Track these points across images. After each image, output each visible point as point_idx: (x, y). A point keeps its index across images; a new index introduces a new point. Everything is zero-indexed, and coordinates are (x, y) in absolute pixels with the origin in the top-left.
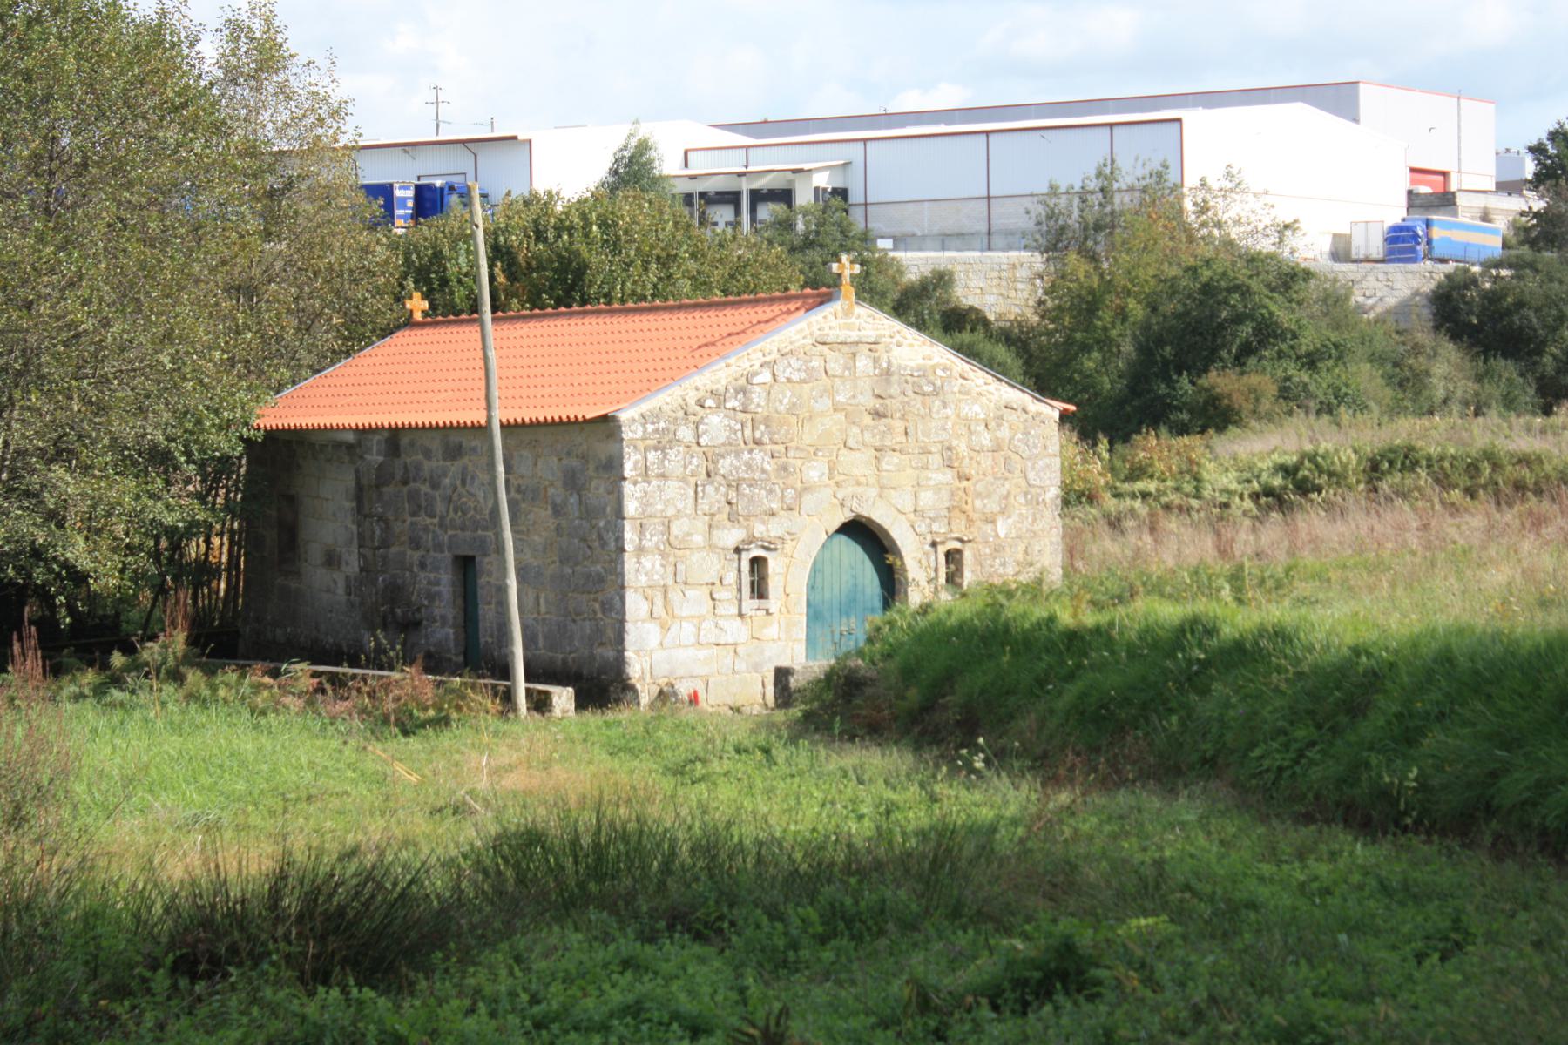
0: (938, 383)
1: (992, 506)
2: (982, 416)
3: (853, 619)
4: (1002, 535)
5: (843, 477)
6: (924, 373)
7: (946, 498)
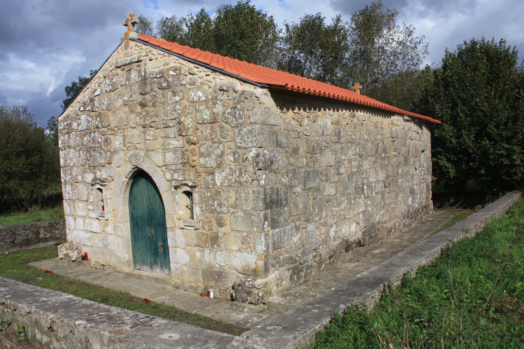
0: (170, 79)
1: (211, 162)
2: (204, 98)
3: (153, 229)
4: (218, 184)
5: (129, 145)
6: (162, 75)
7: (180, 156)
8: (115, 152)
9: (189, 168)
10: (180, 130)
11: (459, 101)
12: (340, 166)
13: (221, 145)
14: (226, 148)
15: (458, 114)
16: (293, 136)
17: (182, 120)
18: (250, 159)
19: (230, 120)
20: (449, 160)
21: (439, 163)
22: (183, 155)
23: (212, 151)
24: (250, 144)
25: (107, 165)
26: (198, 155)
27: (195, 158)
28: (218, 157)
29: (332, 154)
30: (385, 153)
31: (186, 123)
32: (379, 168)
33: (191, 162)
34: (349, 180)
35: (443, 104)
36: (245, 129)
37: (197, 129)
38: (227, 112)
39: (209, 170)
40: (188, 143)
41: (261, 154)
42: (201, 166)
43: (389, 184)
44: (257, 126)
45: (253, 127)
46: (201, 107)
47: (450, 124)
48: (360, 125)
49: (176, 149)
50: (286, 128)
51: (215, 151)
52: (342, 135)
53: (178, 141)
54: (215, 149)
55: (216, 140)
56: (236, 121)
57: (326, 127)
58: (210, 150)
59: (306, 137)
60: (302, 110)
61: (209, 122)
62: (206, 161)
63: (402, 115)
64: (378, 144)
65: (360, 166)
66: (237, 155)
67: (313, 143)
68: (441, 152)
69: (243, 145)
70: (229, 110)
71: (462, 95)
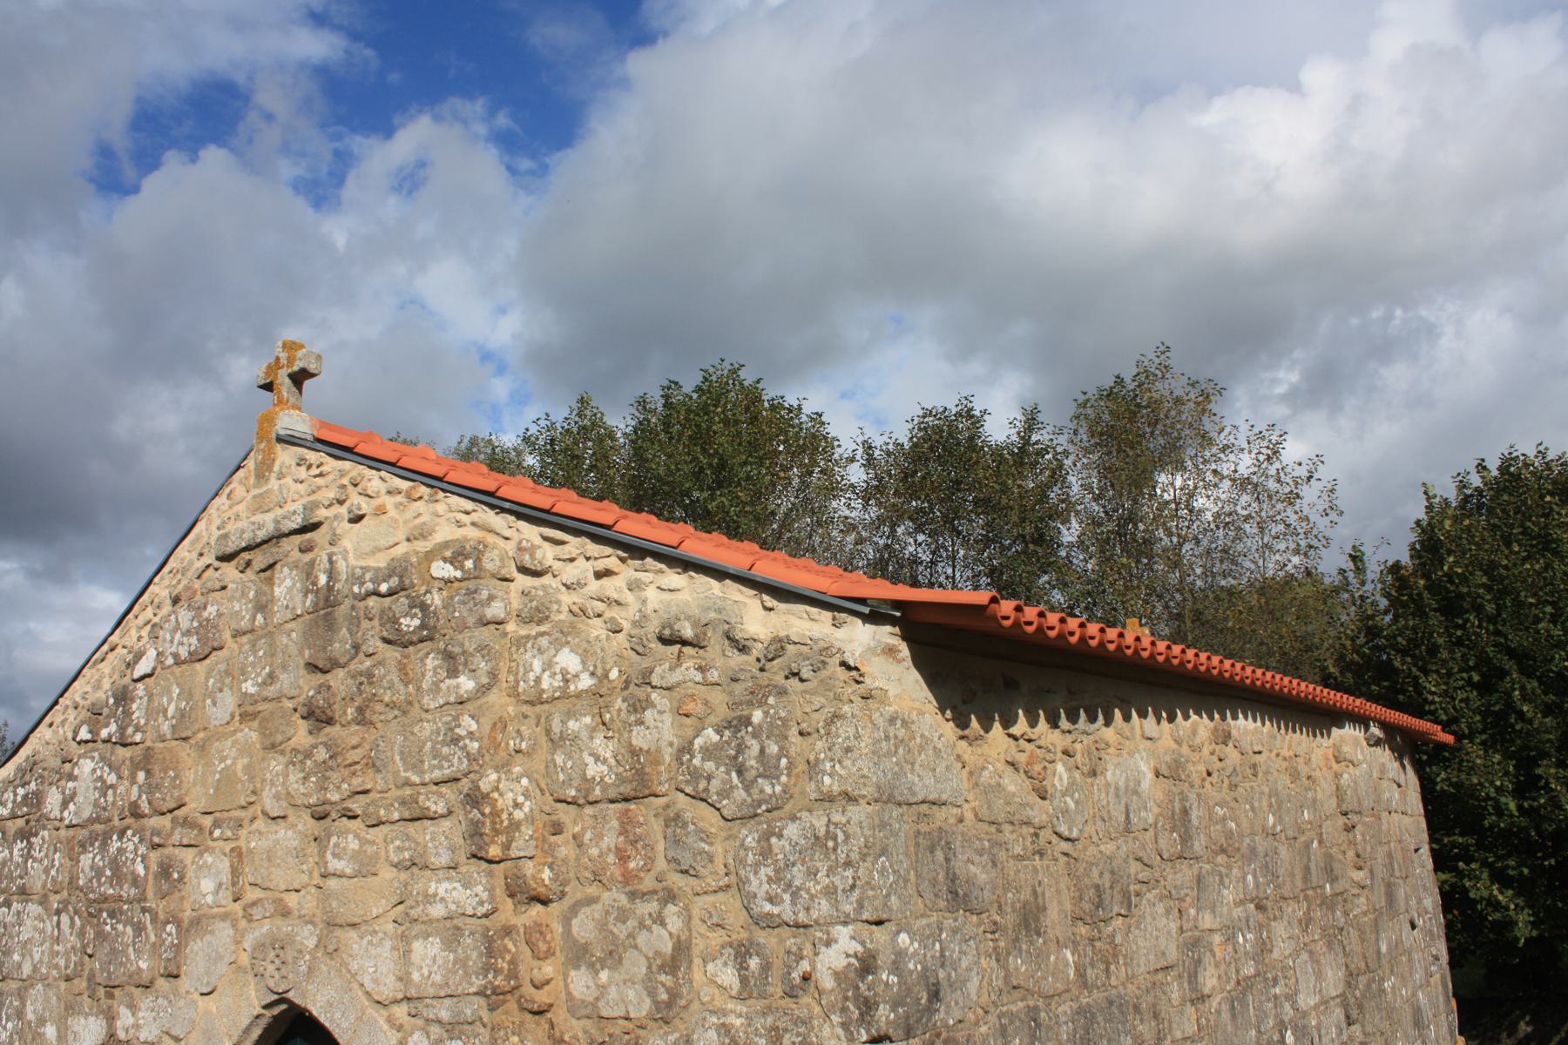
0: (436, 599)
2: (586, 682)
6: (401, 582)
7: (475, 958)
8: (198, 924)
9: (517, 1016)
10: (475, 832)
11: (1509, 664)
12: (1199, 961)
13: (671, 908)
14: (696, 921)
15: (1510, 706)
16: (1018, 850)
17: (485, 785)
18: (828, 983)
19: (715, 784)
20: (1500, 877)
21: (1465, 891)
22: (490, 952)
23: (631, 935)
24: (823, 907)
25: (161, 983)
26: (560, 957)
27: (548, 969)
28: (662, 968)
29: (1168, 911)
30: (1333, 880)
31: (504, 802)
32: (1320, 947)
33: (528, 990)
34: (1234, 1017)
35: (1449, 674)
36: (792, 830)
37: (557, 829)
38: (698, 742)
39: (617, 1031)
40: (511, 896)
41: (884, 959)
42: (574, 1006)
43: (1361, 1007)
44: (857, 813)
45: (837, 818)
46: (572, 725)
47: (1483, 743)
48: (1249, 772)
49: (458, 922)
50: (984, 813)
51: (642, 938)
52: (1195, 822)
53: (467, 885)
54: (642, 925)
55: (648, 883)
56: (747, 789)
57: (1136, 792)
58: (621, 931)
59: (1065, 846)
60: (1043, 724)
61: (612, 794)
62: (603, 988)
63: (1362, 720)
64: (1308, 845)
65: (1264, 948)
66: (754, 963)
67: (1095, 872)
68: (1465, 848)
69: (785, 910)
70: (711, 735)
71: (1515, 639)
